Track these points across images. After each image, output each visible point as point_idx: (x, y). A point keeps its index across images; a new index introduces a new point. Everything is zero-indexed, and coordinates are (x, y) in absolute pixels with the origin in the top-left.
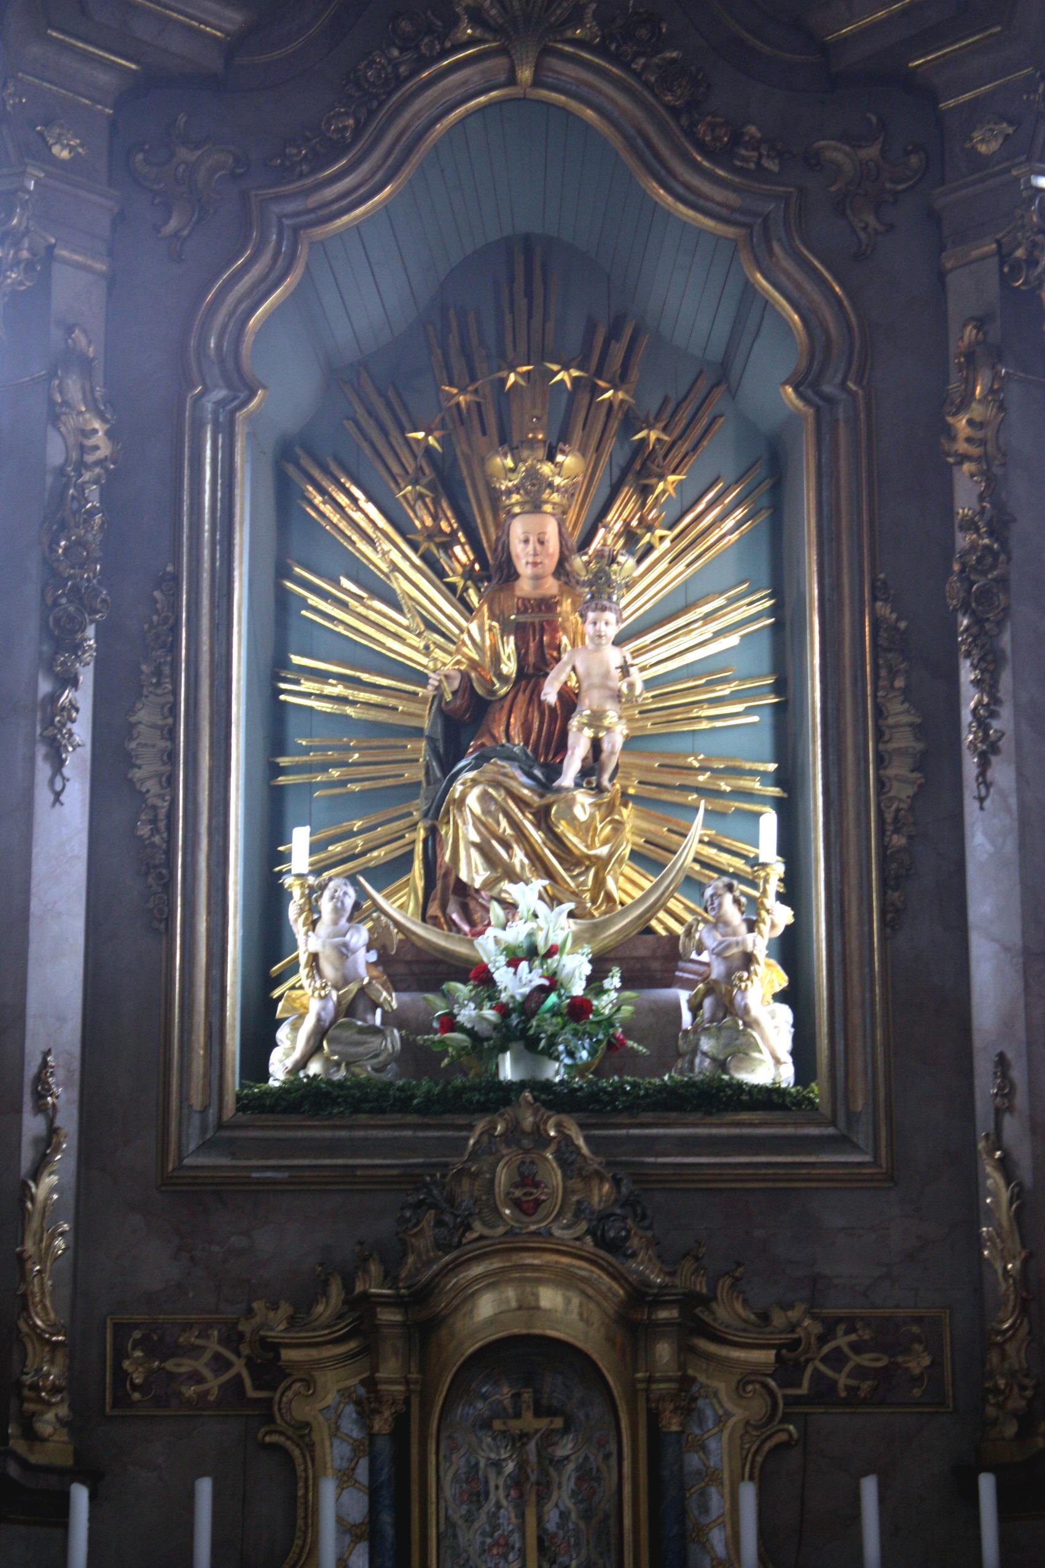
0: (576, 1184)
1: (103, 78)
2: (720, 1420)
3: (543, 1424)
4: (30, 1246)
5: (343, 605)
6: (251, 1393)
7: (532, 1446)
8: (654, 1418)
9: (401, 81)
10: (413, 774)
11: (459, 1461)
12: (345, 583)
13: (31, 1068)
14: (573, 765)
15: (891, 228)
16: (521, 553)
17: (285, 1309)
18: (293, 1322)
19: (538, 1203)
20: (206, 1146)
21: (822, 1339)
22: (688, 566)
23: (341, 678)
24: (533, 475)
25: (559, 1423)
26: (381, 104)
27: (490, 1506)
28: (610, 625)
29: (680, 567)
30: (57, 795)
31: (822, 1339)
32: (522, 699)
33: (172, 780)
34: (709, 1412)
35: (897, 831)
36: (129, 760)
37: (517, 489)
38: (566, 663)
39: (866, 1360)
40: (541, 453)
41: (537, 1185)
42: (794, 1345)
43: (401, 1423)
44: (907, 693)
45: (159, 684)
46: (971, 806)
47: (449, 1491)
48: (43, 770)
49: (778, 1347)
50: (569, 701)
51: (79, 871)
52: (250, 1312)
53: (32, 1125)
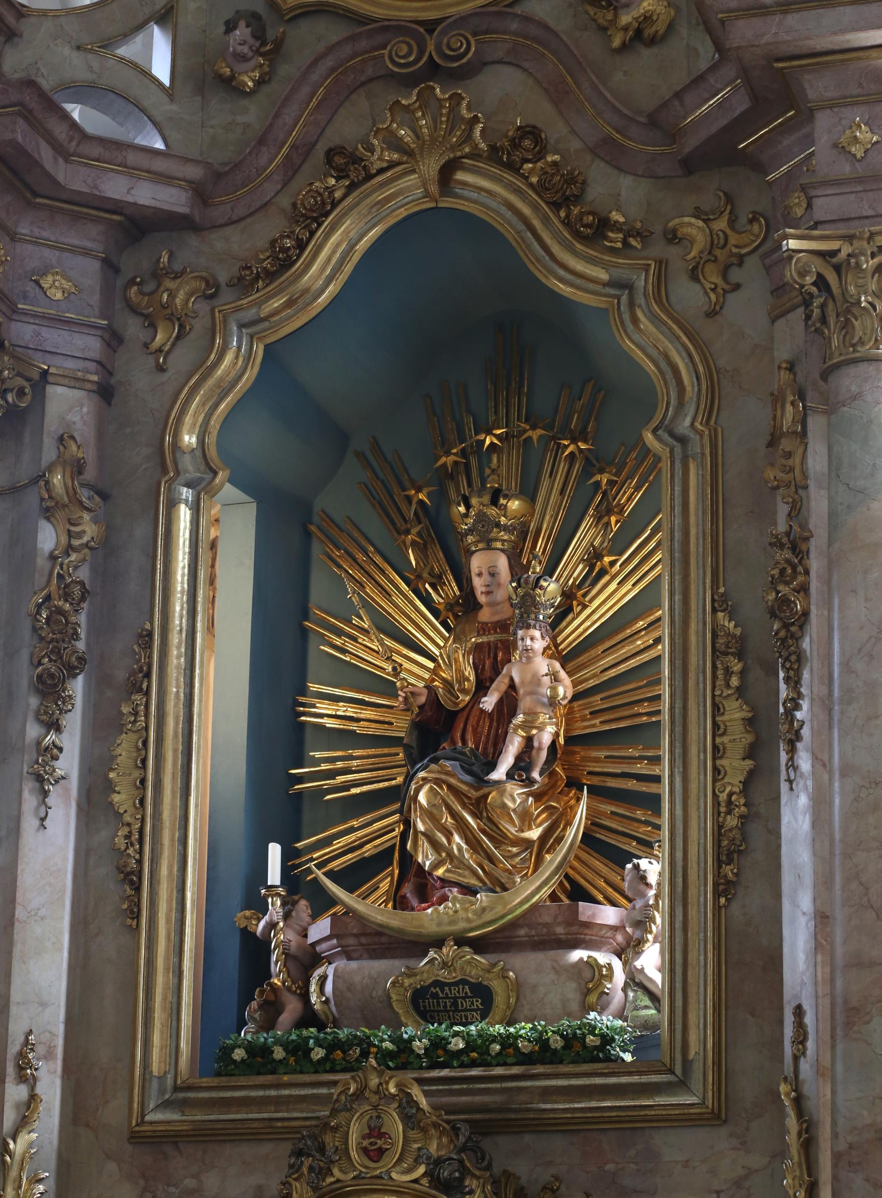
9: (335, 204)
13: (13, 1049)
15: (737, 287)
19: (381, 1152)
20: (165, 1105)
22: (634, 585)
26: (319, 225)
29: (628, 585)
30: (43, 819)
35: (729, 812)
36: (110, 788)
38: (505, 676)
41: (381, 1135)
45: (135, 721)
48: (29, 800)
53: (15, 1092)
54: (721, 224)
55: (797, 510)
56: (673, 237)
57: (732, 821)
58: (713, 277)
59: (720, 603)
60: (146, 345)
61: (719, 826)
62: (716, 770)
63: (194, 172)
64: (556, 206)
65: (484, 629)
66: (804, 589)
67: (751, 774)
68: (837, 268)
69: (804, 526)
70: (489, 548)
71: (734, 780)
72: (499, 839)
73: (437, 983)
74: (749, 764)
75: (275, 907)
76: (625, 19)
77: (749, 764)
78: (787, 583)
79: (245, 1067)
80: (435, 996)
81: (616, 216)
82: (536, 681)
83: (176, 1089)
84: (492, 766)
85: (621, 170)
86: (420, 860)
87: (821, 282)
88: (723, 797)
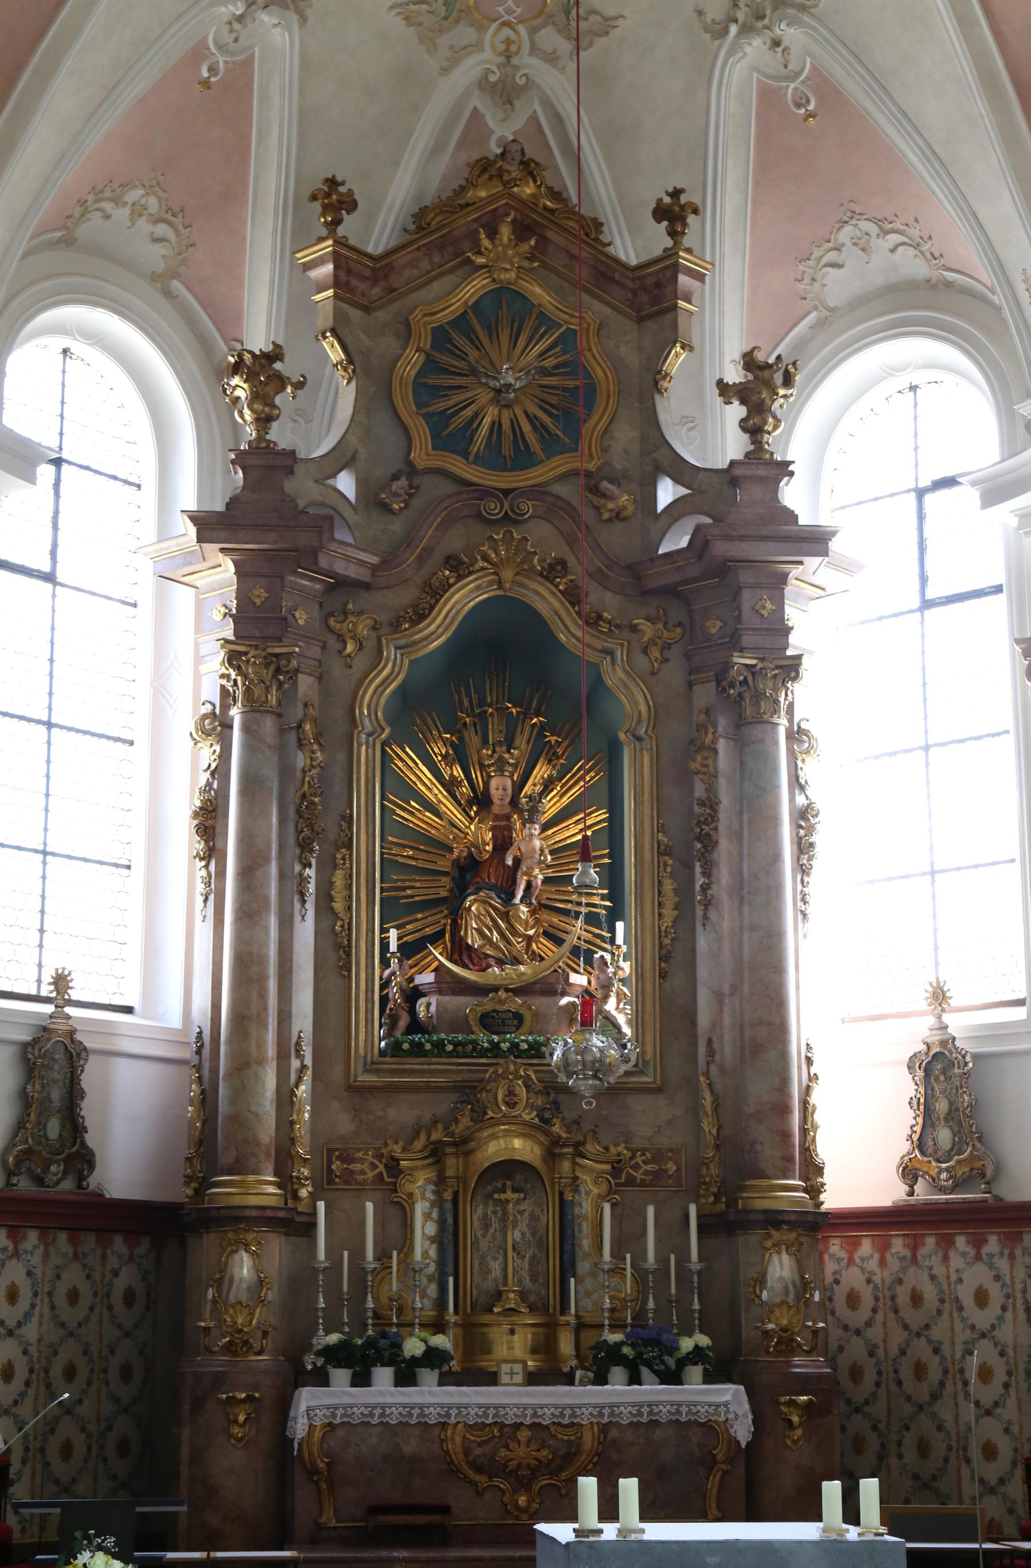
0: (531, 1095)
1: (318, 586)
2: (588, 1193)
3: (515, 1196)
4: (295, 1117)
5: (412, 814)
6: (387, 1179)
7: (511, 1205)
8: (561, 1194)
9: (450, 586)
10: (444, 893)
11: (480, 1211)
12: (413, 803)
13: (294, 1040)
14: (520, 894)
15: (667, 660)
16: (495, 794)
17: (401, 1143)
18: (404, 1149)
19: (516, 1103)
20: (366, 1071)
21: (631, 1159)
23: (411, 848)
24: (501, 759)
25: (522, 1196)
26: (442, 596)
27: (491, 1231)
28: (536, 829)
29: (565, 799)
30: (303, 916)
31: (631, 1159)
32: (495, 861)
33: (350, 908)
34: (583, 1190)
35: (666, 936)
36: (331, 899)
37: (492, 765)
39: (648, 1167)
40: (504, 749)
41: (515, 1095)
42: (619, 1162)
43: (456, 1194)
44: (672, 875)
45: (344, 864)
46: (699, 926)
47: (476, 1224)
48: (297, 905)
49: (612, 1163)
50: (517, 861)
51: (310, 949)
52: (386, 1145)
54: (660, 626)
55: (711, 789)
56: (634, 629)
57: (667, 941)
58: (655, 653)
59: (661, 829)
60: (340, 652)
61: (661, 943)
62: (660, 915)
63: (374, 560)
64: (573, 605)
65: (497, 818)
66: (716, 829)
67: (677, 917)
68: (753, 674)
69: (716, 796)
70: (503, 775)
71: (668, 921)
72: (515, 933)
73: (494, 1011)
74: (676, 912)
75: (394, 962)
76: (611, 505)
77: (676, 912)
78: (707, 825)
79: (409, 1053)
80: (493, 1017)
81: (606, 615)
82: (534, 851)
83: (372, 1063)
84: (513, 896)
85: (606, 588)
86: (470, 942)
87: (745, 681)
88: (663, 928)
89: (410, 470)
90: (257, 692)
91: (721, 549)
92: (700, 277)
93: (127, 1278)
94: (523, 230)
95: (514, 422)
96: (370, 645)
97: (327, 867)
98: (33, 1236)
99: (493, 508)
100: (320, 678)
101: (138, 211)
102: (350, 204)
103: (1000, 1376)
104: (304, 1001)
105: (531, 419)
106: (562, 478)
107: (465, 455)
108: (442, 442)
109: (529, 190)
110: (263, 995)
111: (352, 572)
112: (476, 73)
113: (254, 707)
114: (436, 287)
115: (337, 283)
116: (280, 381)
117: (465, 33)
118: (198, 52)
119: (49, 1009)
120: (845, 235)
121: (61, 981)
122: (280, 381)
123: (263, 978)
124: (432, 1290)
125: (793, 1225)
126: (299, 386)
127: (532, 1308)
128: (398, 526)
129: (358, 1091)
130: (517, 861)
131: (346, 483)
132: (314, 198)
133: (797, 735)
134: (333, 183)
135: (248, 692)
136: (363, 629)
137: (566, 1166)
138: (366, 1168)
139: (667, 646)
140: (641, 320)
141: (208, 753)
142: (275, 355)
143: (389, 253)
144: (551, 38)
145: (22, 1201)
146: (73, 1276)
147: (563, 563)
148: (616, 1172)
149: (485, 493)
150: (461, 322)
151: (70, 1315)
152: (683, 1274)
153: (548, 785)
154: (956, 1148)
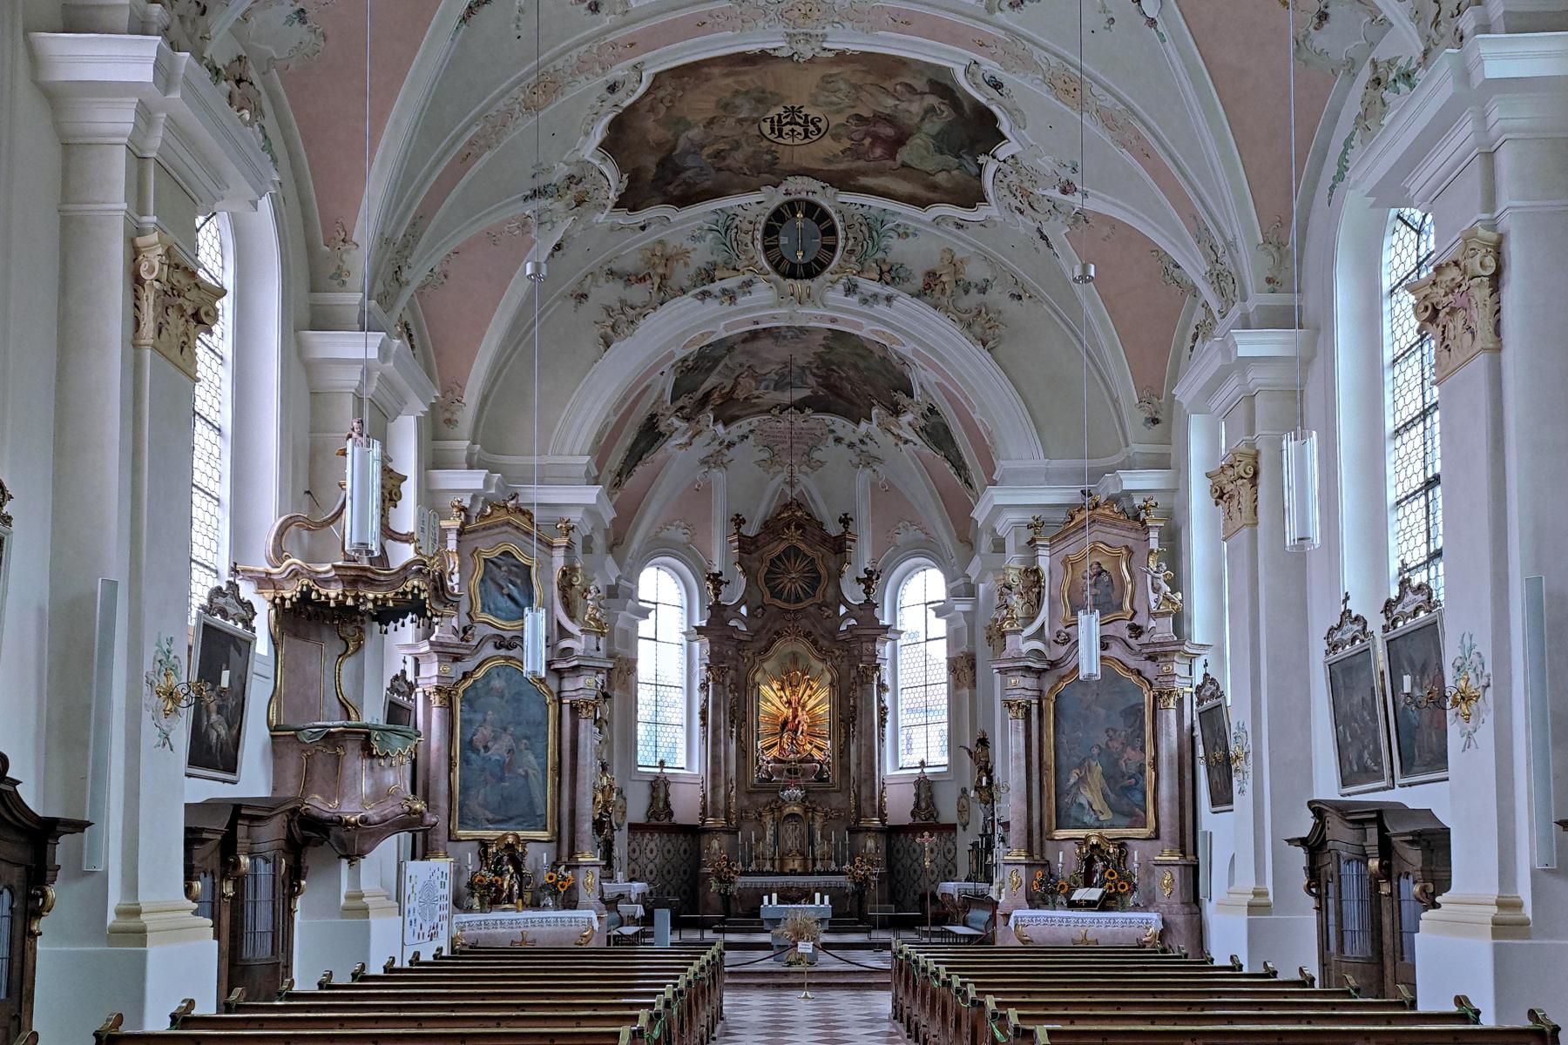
50: (799, 722)
89: (763, 606)
90: (717, 678)
91: (855, 632)
92: (854, 541)
93: (685, 845)
94: (798, 527)
95: (796, 589)
96: (752, 660)
97: (739, 727)
98: (657, 835)
99: (788, 616)
100: (737, 670)
101: (678, 527)
102: (744, 521)
103: (936, 872)
104: (733, 767)
105: (801, 587)
106: (811, 605)
107: (780, 599)
108: (773, 595)
109: (799, 514)
110: (720, 767)
111: (745, 638)
112: (782, 480)
113: (716, 682)
114: (771, 546)
115: (739, 548)
116: (721, 583)
117: (778, 468)
118: (695, 481)
119: (658, 770)
120: (900, 525)
121: (662, 763)
122: (721, 583)
123: (720, 762)
124: (772, 850)
125: (873, 831)
126: (728, 583)
127: (801, 855)
128: (760, 622)
129: (750, 793)
130: (799, 722)
131: (744, 610)
132: (732, 520)
133: (882, 687)
134: (738, 515)
135: (713, 679)
136: (750, 655)
137: (810, 814)
138: (752, 815)
139: (843, 657)
140: (836, 553)
141: (703, 696)
142: (721, 574)
143: (756, 536)
144: (804, 468)
145: (653, 826)
146: (669, 846)
147: (810, 632)
148: (826, 816)
149: (788, 611)
150: (779, 557)
151: (669, 857)
152: (844, 845)
153: (810, 697)
154: (927, 808)
